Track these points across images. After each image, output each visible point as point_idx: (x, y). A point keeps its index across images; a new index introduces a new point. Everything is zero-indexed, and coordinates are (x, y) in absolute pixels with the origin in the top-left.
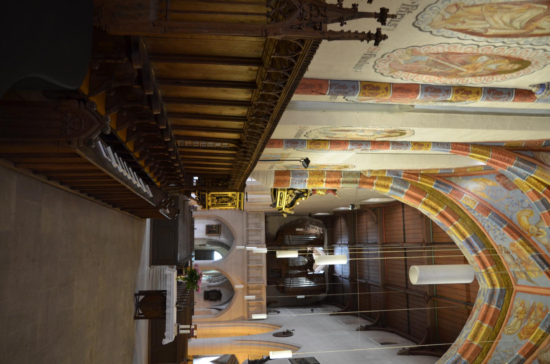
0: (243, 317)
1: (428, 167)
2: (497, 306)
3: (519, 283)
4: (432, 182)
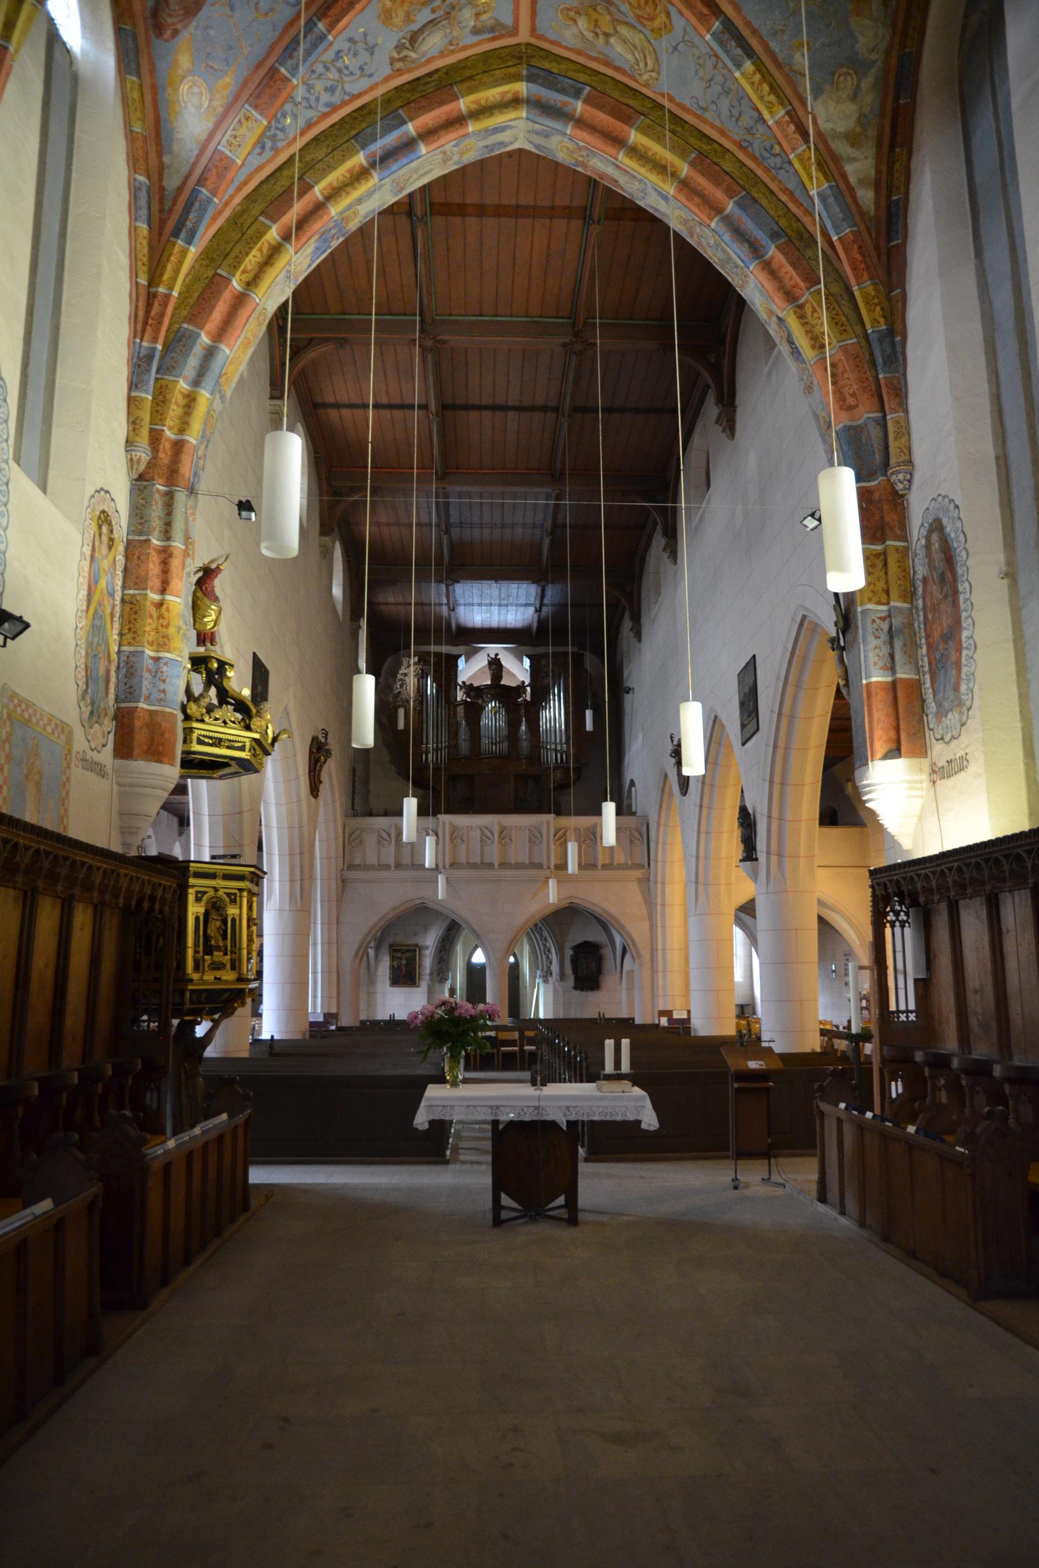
0: (640, 881)
1: (123, 259)
2: (577, 95)
3: (508, 21)
4: (176, 250)
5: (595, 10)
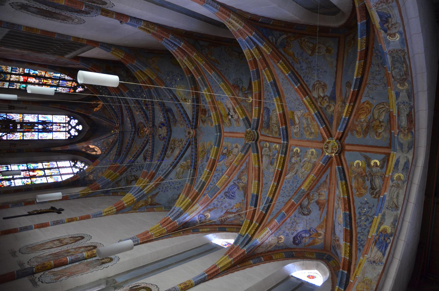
3: (383, 156)
5: (374, 127)
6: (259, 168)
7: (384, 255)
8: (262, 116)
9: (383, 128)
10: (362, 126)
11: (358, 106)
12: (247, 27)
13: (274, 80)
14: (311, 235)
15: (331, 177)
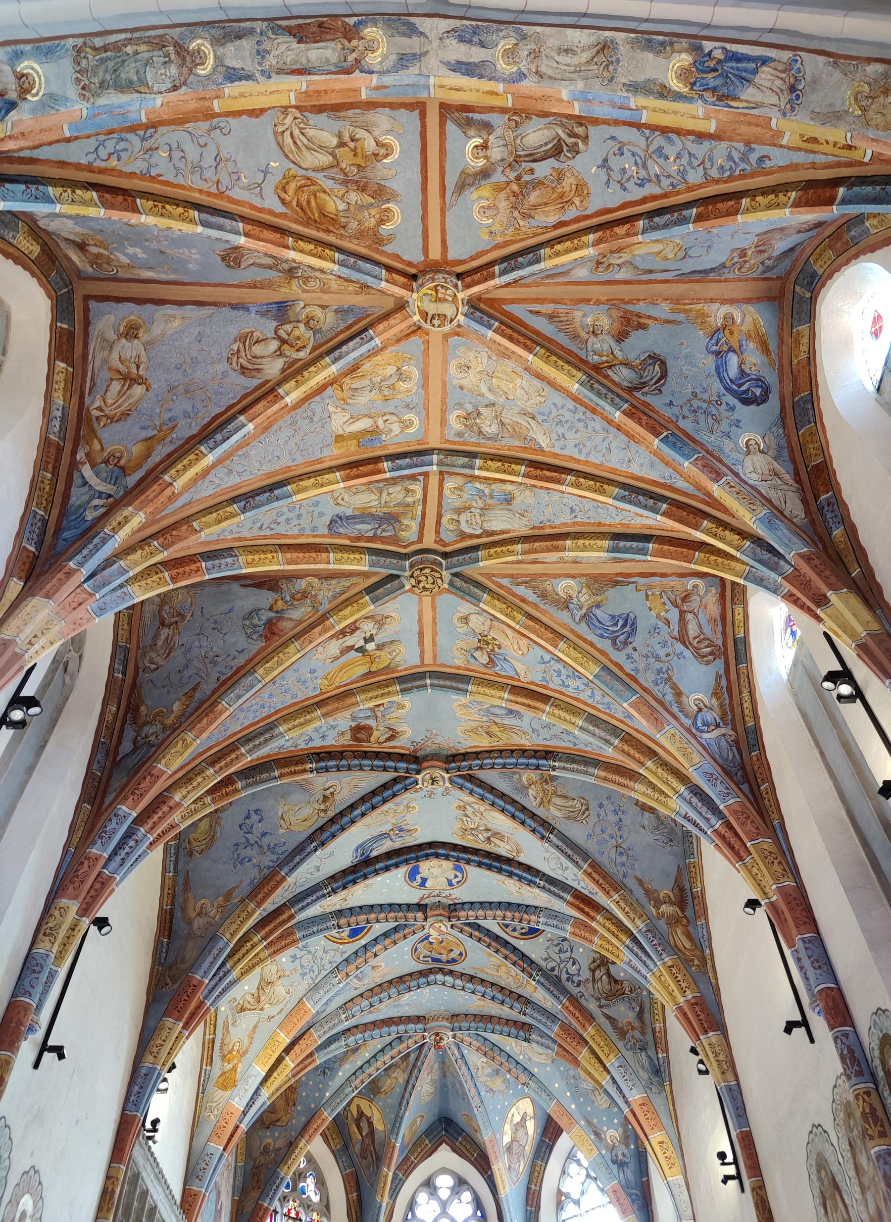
3: (451, 128)
6: (526, 539)
7: (765, 61)
8: (358, 539)
9: (360, 133)
10: (361, 207)
11: (296, 222)
12: (49, 586)
13: (233, 500)
14: (731, 349)
15: (537, 301)
